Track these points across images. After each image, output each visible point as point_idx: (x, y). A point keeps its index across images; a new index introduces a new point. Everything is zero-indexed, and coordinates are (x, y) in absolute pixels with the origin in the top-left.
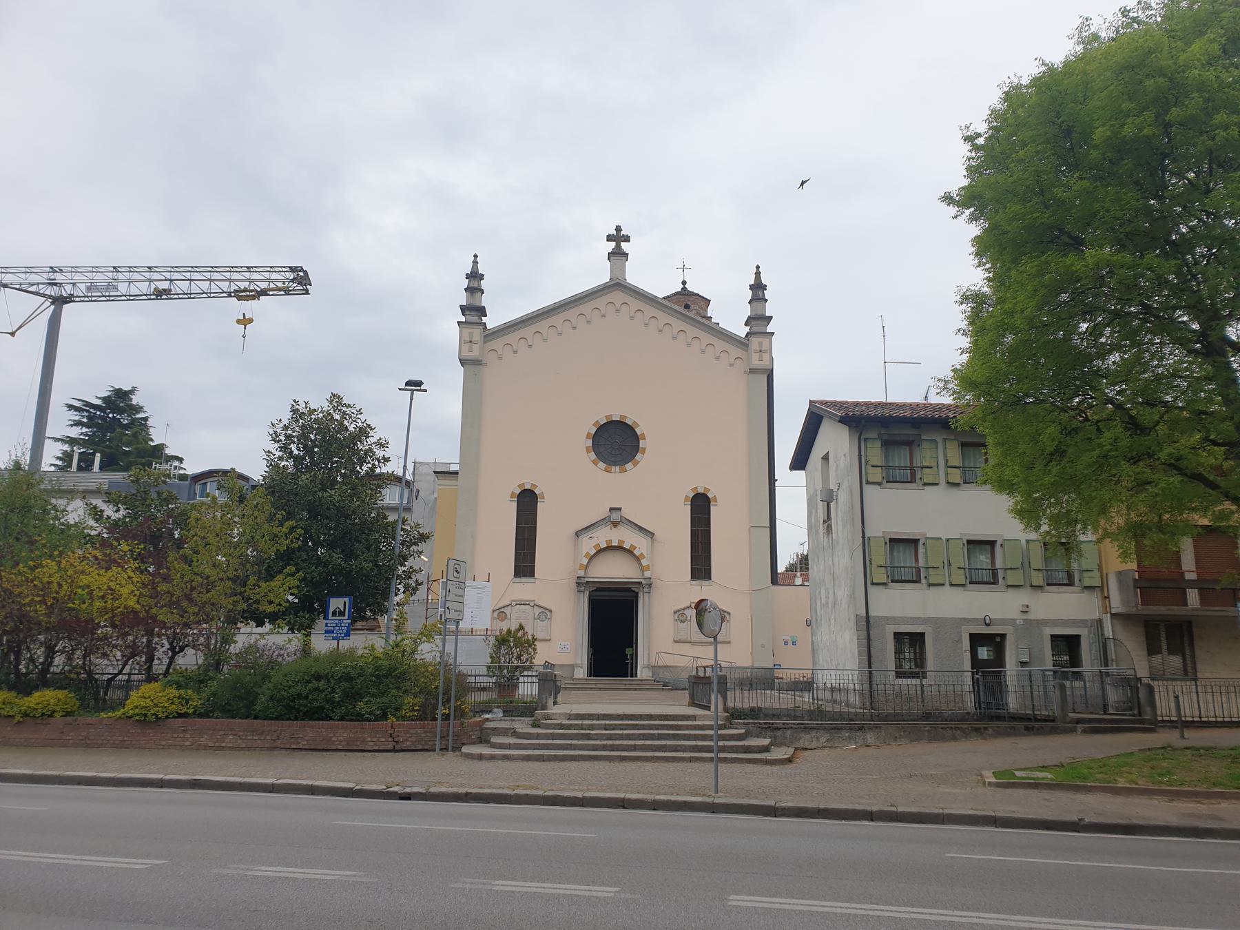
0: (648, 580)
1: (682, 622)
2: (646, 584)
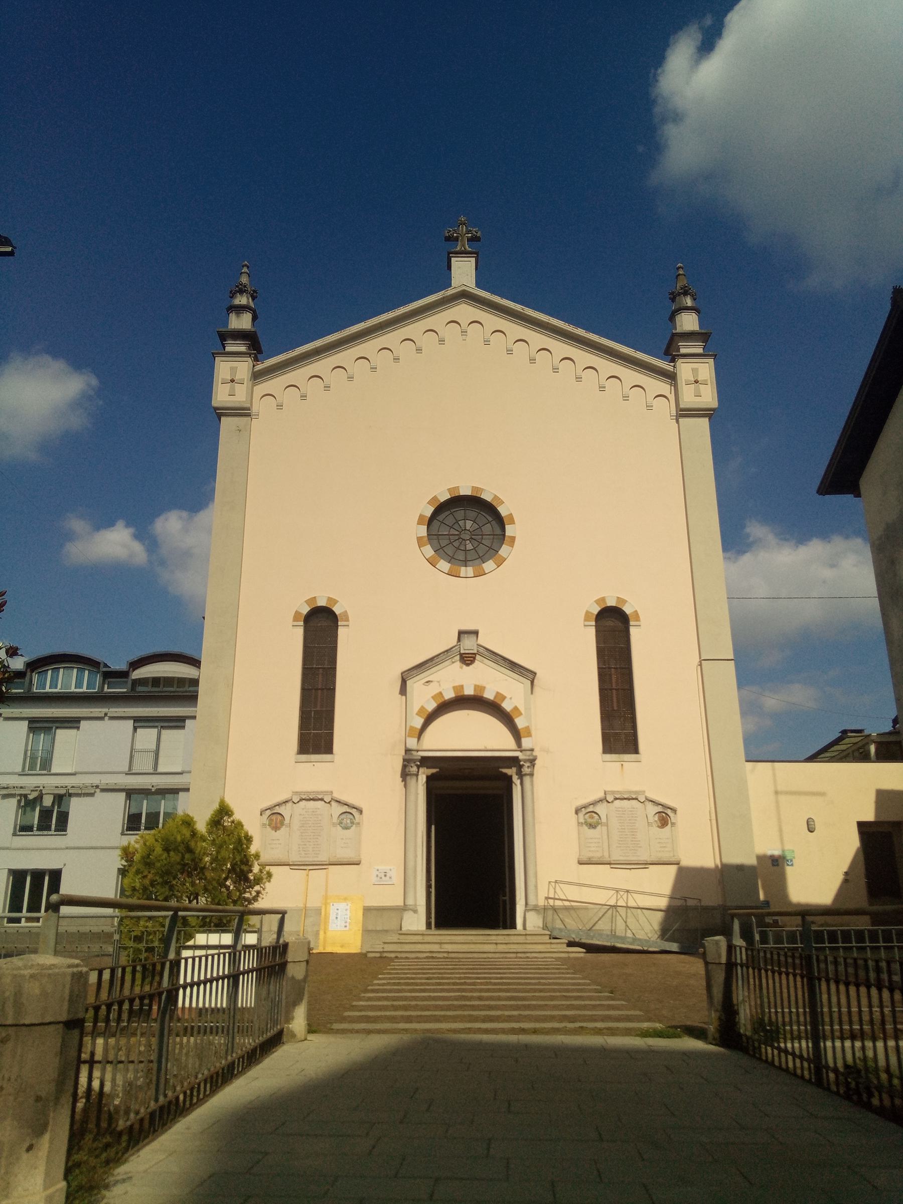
0: (529, 753)
1: (592, 826)
2: (525, 761)
